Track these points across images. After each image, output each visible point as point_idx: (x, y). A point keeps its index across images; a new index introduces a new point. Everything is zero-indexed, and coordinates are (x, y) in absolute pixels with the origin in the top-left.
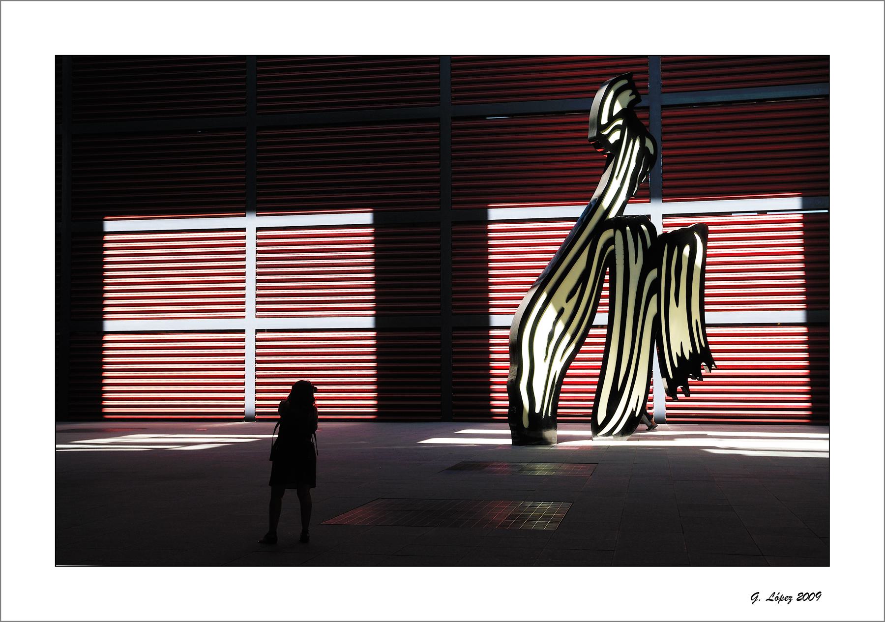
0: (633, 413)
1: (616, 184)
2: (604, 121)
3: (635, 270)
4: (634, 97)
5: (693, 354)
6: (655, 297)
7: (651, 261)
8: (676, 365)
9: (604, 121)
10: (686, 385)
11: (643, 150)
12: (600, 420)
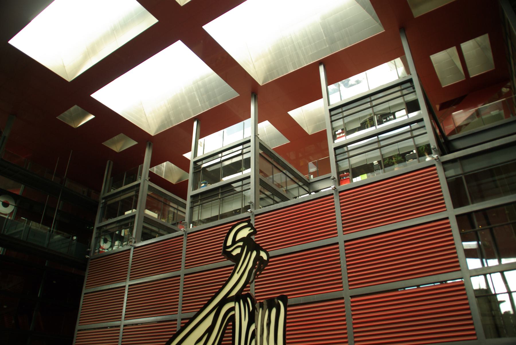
1: (236, 277)
2: (229, 243)
3: (245, 324)
4: (252, 231)
7: (252, 320)
9: (229, 243)
11: (258, 258)
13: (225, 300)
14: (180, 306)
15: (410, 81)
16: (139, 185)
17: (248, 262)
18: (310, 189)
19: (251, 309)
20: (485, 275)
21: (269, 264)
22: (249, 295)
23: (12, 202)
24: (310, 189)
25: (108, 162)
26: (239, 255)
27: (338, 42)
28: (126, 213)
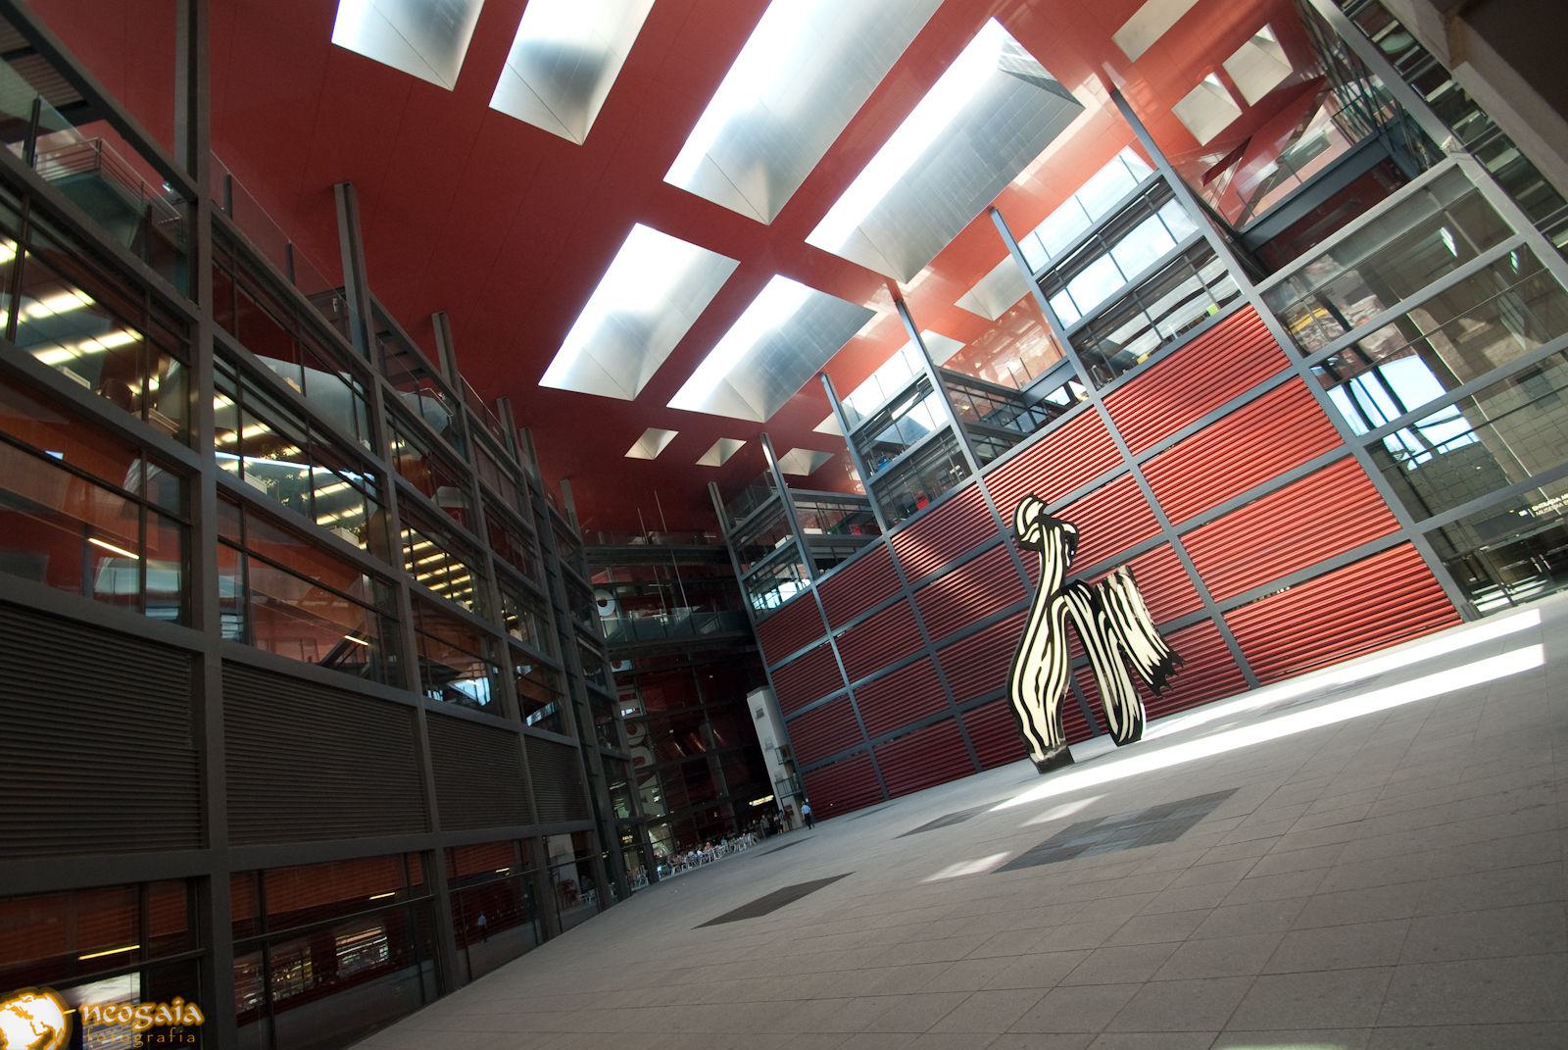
0: (1135, 718)
3: (1089, 616)
4: (1041, 505)
5: (1162, 660)
6: (1110, 631)
7: (1096, 607)
8: (1151, 673)
9: (1022, 531)
10: (1165, 683)
11: (1065, 535)
12: (1116, 731)
13: (1050, 600)
14: (835, 648)
15: (1161, 179)
16: (779, 498)
17: (1054, 543)
18: (1025, 404)
19: (1089, 596)
20: (1395, 433)
21: (1081, 539)
22: (1078, 582)
23: (607, 597)
24: (1025, 404)
25: (709, 484)
26: (1041, 540)
27: (1011, 163)
28: (778, 545)
